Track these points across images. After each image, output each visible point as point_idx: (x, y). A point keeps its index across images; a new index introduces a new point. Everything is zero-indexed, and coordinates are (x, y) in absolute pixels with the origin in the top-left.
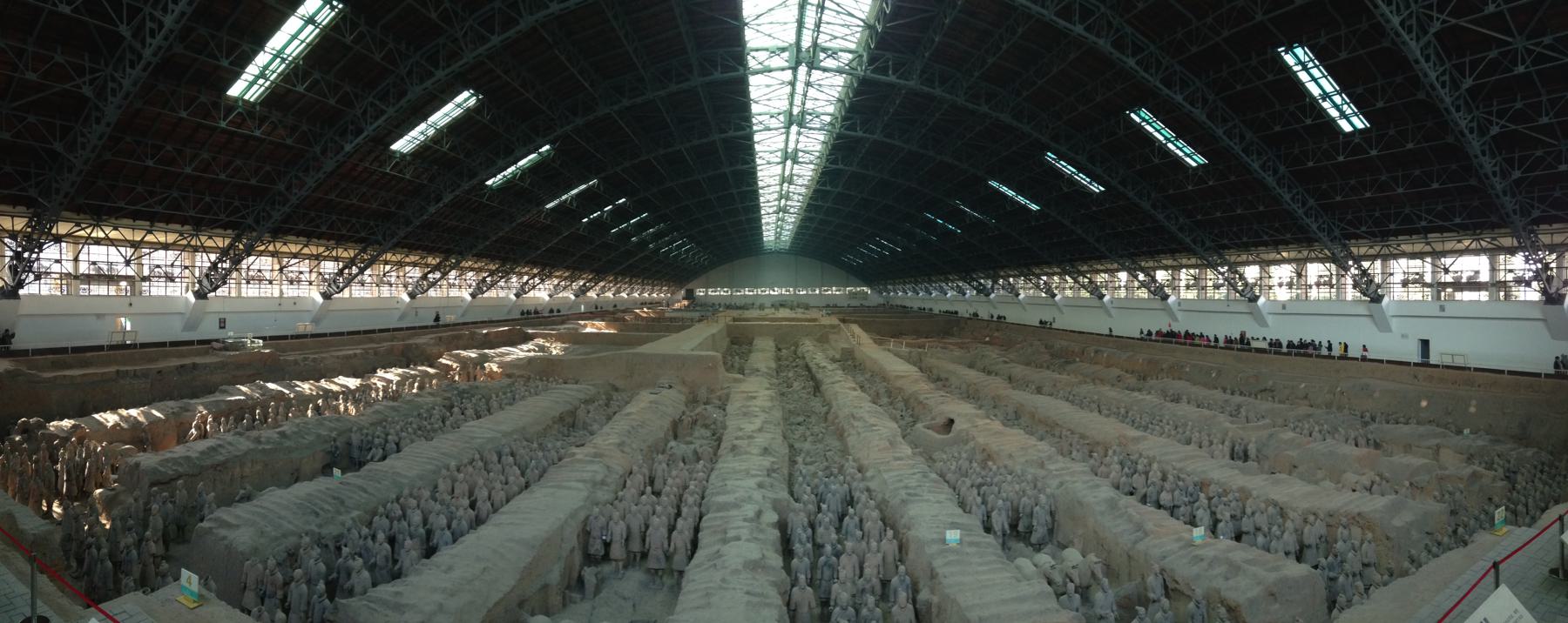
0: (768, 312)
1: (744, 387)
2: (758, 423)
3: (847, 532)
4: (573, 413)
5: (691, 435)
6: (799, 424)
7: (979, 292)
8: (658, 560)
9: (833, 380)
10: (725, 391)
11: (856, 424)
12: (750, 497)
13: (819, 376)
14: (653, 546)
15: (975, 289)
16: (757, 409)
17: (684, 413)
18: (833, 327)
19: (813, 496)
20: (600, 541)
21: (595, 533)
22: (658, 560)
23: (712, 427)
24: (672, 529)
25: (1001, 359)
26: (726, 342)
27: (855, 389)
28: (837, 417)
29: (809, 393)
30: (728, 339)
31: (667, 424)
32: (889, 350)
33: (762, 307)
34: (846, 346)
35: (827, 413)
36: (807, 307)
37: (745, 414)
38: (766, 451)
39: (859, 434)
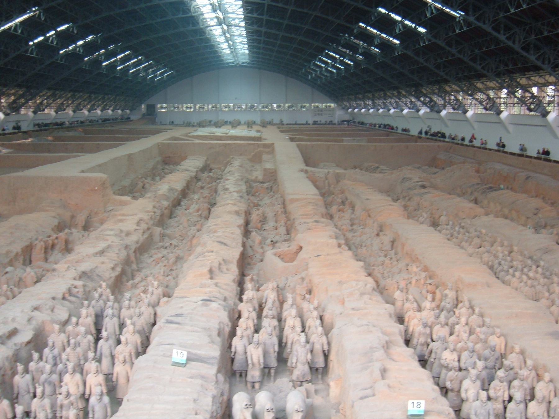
0: (219, 132)
2: (102, 245)
3: (101, 354)
7: (432, 108)
13: (218, 199)
15: (424, 103)
19: (90, 320)
25: (420, 183)
27: (237, 213)
29: (200, 216)
30: (159, 159)
31: (17, 248)
32: (306, 172)
33: (218, 125)
38: (84, 275)
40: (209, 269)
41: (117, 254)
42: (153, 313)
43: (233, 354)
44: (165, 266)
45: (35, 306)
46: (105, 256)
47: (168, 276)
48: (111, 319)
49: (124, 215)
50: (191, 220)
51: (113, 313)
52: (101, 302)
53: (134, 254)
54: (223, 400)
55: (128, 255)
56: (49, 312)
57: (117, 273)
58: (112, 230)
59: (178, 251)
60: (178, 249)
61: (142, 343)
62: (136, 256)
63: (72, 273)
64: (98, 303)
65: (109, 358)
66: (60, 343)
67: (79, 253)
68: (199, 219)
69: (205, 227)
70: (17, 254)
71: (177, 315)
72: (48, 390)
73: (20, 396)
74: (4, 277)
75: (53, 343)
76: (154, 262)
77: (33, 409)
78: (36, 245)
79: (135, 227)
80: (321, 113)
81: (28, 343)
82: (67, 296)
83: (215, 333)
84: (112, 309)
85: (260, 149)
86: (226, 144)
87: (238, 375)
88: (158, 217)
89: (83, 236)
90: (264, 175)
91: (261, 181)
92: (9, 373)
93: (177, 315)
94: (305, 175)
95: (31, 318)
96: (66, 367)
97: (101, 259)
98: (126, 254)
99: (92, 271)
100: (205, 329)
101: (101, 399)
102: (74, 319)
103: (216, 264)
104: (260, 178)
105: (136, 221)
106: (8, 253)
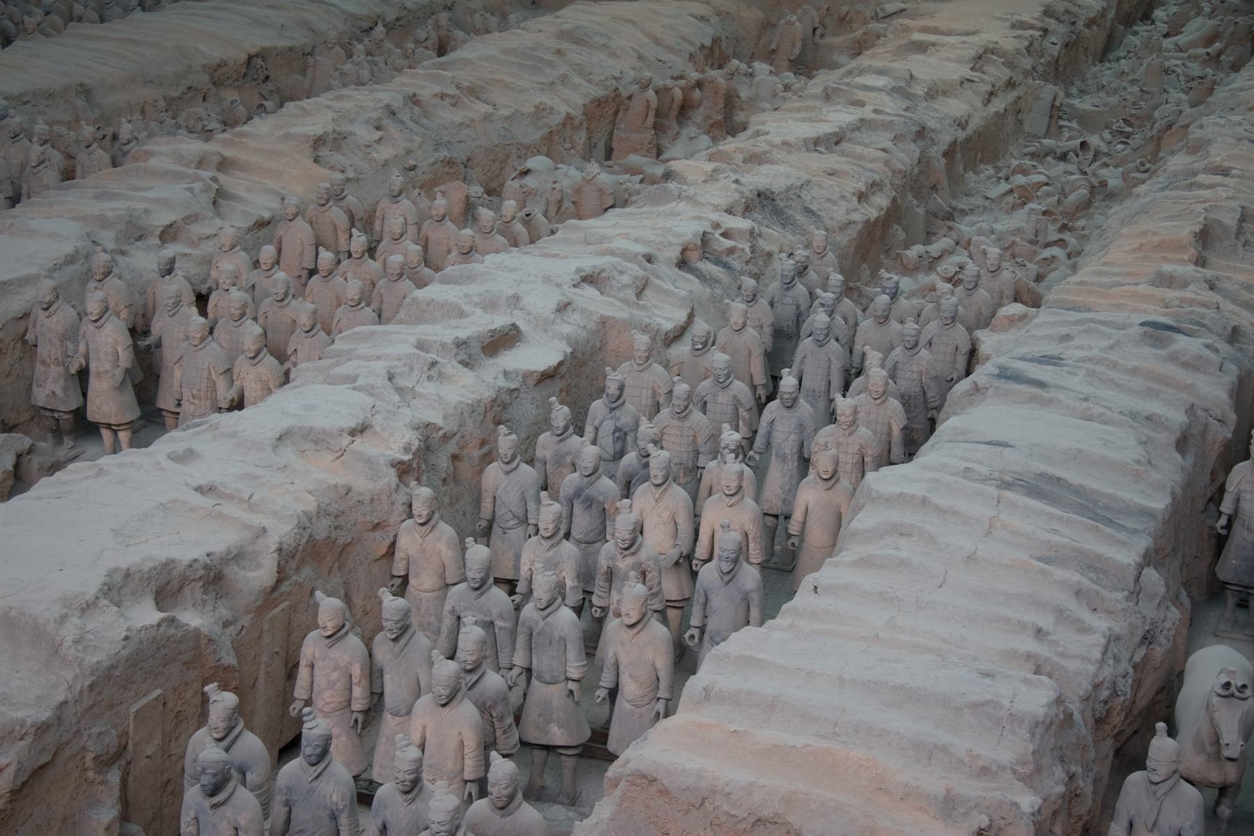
3: (768, 445)
4: (301, 58)
14: (187, 394)
20: (61, 369)
21: (48, 350)
29: (1215, 59)
37: (828, 96)
40: (1197, 229)
41: (884, 150)
42: (965, 348)
43: (1223, 521)
44: (1045, 213)
45: (589, 271)
46: (843, 154)
47: (1048, 245)
48: (820, 344)
49: (935, 31)
50: (1179, 70)
51: (829, 328)
52: (800, 289)
53: (943, 161)
54: (1145, 659)
55: (924, 161)
56: (630, 294)
57: (873, 214)
58: (881, 72)
59: (1103, 172)
60: (1106, 165)
61: (907, 430)
62: (950, 168)
63: (721, 193)
64: (790, 293)
65: (793, 465)
66: (647, 394)
67: (758, 134)
69: (1221, 94)
70: (569, 117)
71: (1046, 360)
72: (583, 522)
73: (496, 530)
74: (516, 184)
75: (621, 388)
76: (1010, 199)
77: (524, 571)
78: (630, 98)
79: (966, 72)
81: (547, 377)
82: (694, 256)
83: (1167, 438)
84: (831, 314)
87: (1231, 601)
88: (1057, 47)
89: (787, 88)
92: (477, 453)
93: (1046, 360)
95: (569, 304)
96: (647, 465)
97: (832, 160)
98: (917, 154)
99: (795, 191)
100: (1133, 415)
101: (730, 576)
102: (700, 327)
103: (1230, 220)
105: (972, 53)
106: (540, 111)
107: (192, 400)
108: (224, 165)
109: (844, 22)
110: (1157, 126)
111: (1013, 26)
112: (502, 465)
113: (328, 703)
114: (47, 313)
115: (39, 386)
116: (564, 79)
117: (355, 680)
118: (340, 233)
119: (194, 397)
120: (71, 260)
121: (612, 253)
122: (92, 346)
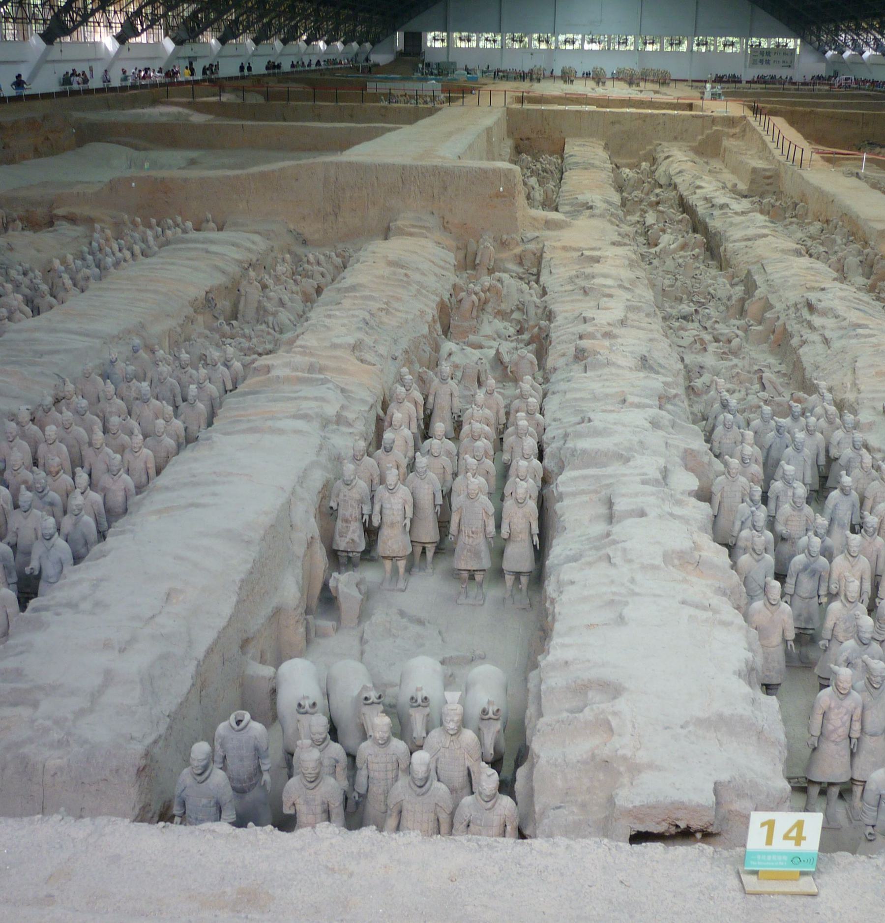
1: (568, 237)
4: (234, 290)
5: (475, 331)
6: (685, 318)
8: (477, 554)
9: (751, 232)
10: (532, 246)
11: (817, 321)
12: (641, 442)
13: (716, 224)
16: (609, 282)
17: (455, 286)
18: (731, 122)
21: (349, 511)
22: (477, 554)
23: (516, 315)
24: (499, 495)
26: (507, 146)
27: (798, 253)
28: (769, 306)
29: (695, 257)
30: (509, 143)
32: (857, 175)
33: (567, 76)
34: (760, 164)
35: (743, 300)
36: (663, 80)
39: (826, 341)
58: (605, 276)
59: (717, 326)
60: (717, 322)
67: (585, 320)
68: (697, 264)
76: (698, 346)
80: (765, 58)
85: (715, 128)
86: (646, 115)
90: (753, 182)
91: (745, 194)
94: (862, 184)
104: (742, 187)
105: (627, 262)
106: (422, 312)
107: (471, 535)
108: (321, 370)
109: (503, 245)
110: (734, 298)
111: (614, 244)
112: (755, 556)
113: (840, 736)
114: (350, 487)
115: (341, 536)
116: (418, 291)
117: (854, 719)
118: (419, 406)
119: (473, 533)
120: (321, 447)
121: (638, 406)
122: (387, 505)
